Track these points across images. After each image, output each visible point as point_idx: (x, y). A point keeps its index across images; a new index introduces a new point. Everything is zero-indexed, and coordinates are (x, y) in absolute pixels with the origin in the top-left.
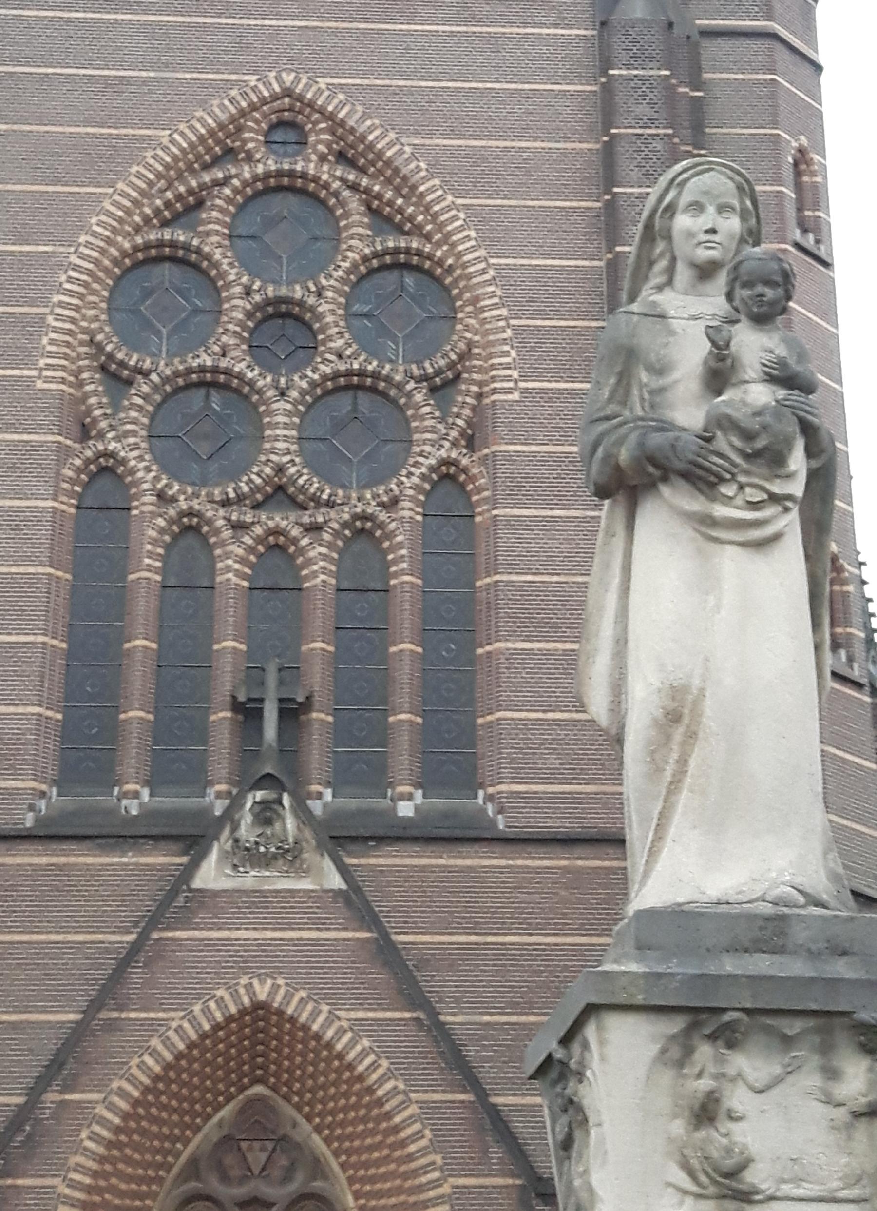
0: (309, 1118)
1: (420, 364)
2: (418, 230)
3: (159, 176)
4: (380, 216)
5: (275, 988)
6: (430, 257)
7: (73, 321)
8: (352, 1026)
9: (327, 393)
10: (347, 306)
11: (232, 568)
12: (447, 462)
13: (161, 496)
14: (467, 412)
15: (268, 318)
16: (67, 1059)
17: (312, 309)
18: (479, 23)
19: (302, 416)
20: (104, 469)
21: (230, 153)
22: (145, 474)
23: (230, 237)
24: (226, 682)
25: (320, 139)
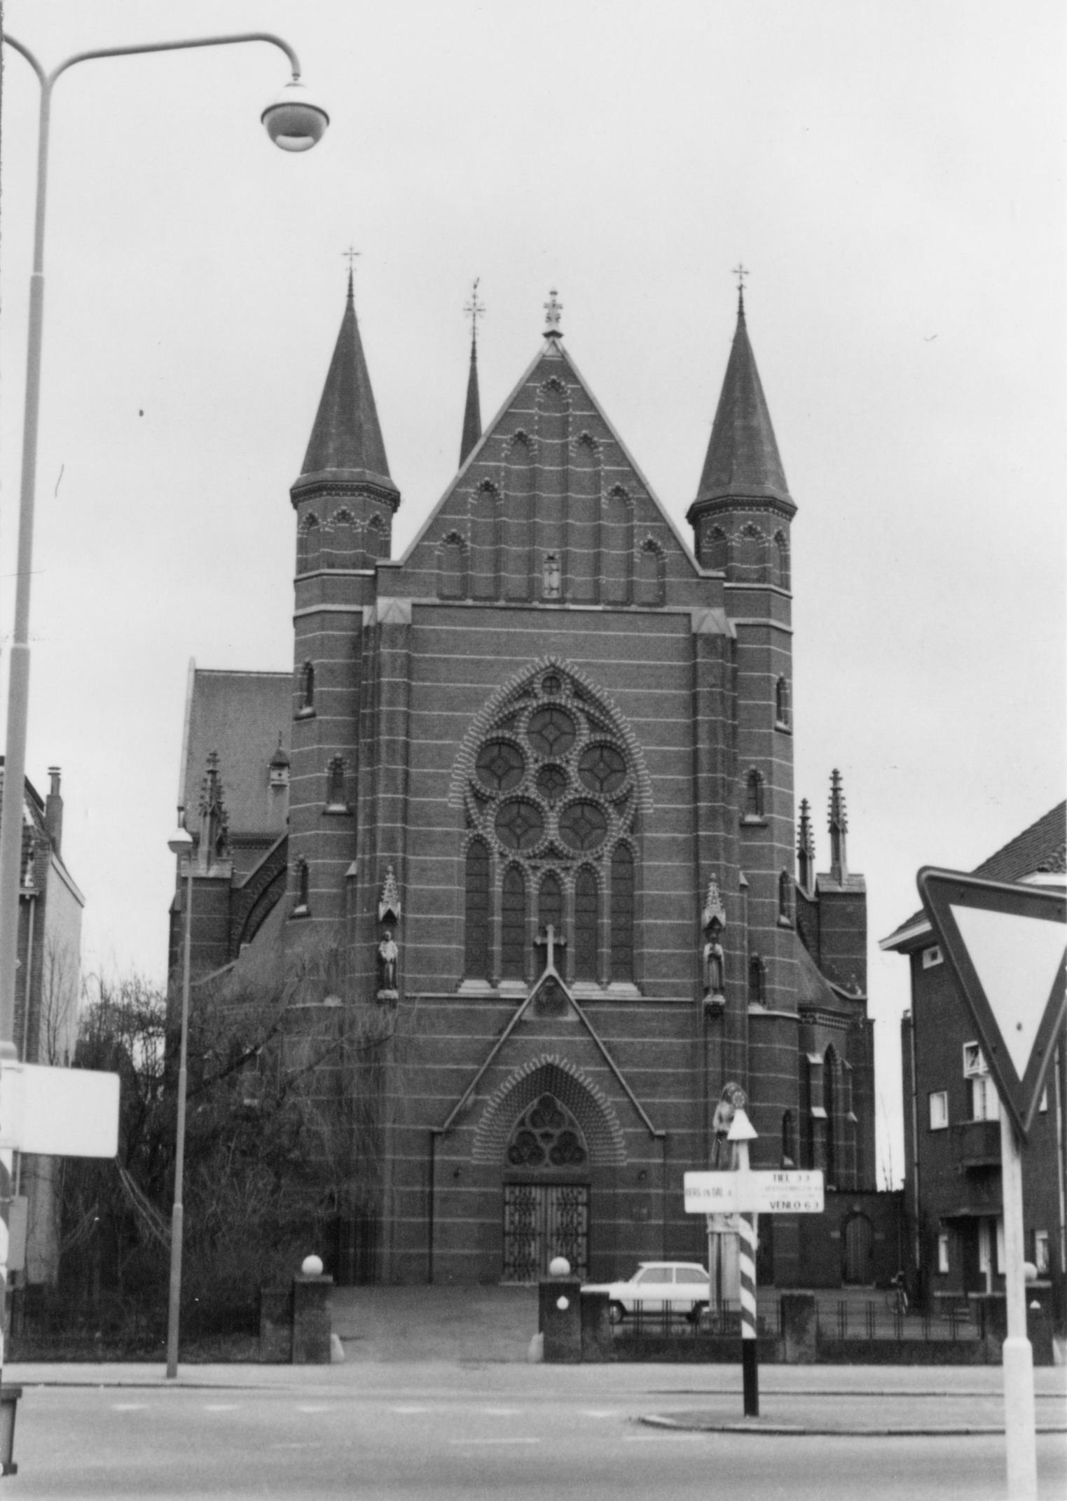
2: (609, 731)
4: (595, 725)
11: (533, 885)
12: (623, 840)
13: (502, 855)
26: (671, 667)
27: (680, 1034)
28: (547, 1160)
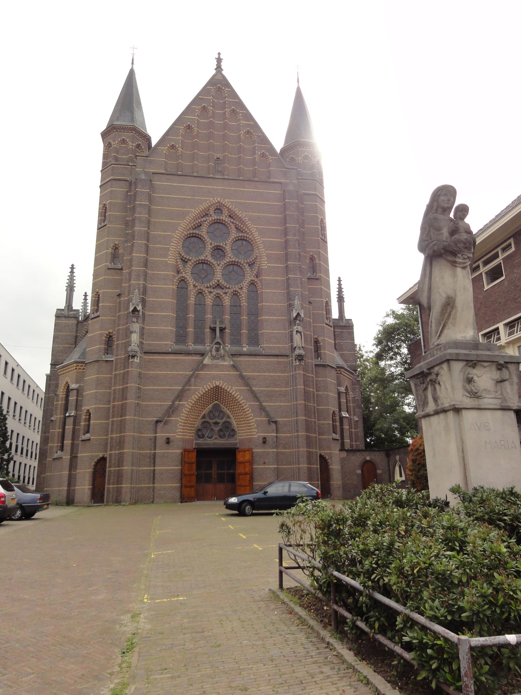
0: (226, 407)
1: (247, 260)
5: (220, 383)
6: (248, 238)
7: (175, 249)
8: (235, 390)
9: (227, 265)
10: (231, 248)
11: (209, 300)
12: (252, 280)
13: (194, 286)
14: (256, 270)
15: (215, 249)
16: (180, 396)
17: (224, 248)
18: (258, 189)
19: (223, 270)
20: (182, 280)
22: (191, 281)
24: (209, 323)
25: (226, 212)
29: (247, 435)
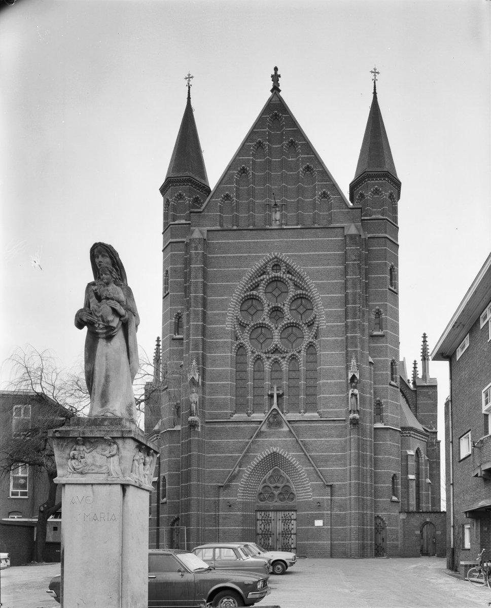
2: (304, 289)
3: (249, 279)
4: (297, 286)
6: (307, 295)
8: (291, 456)
11: (267, 365)
12: (311, 342)
13: (253, 352)
21: (264, 273)
22: (249, 348)
23: (265, 293)
25: (283, 268)
26: (335, 255)
27: (338, 436)
28: (276, 499)
29: (304, 498)
